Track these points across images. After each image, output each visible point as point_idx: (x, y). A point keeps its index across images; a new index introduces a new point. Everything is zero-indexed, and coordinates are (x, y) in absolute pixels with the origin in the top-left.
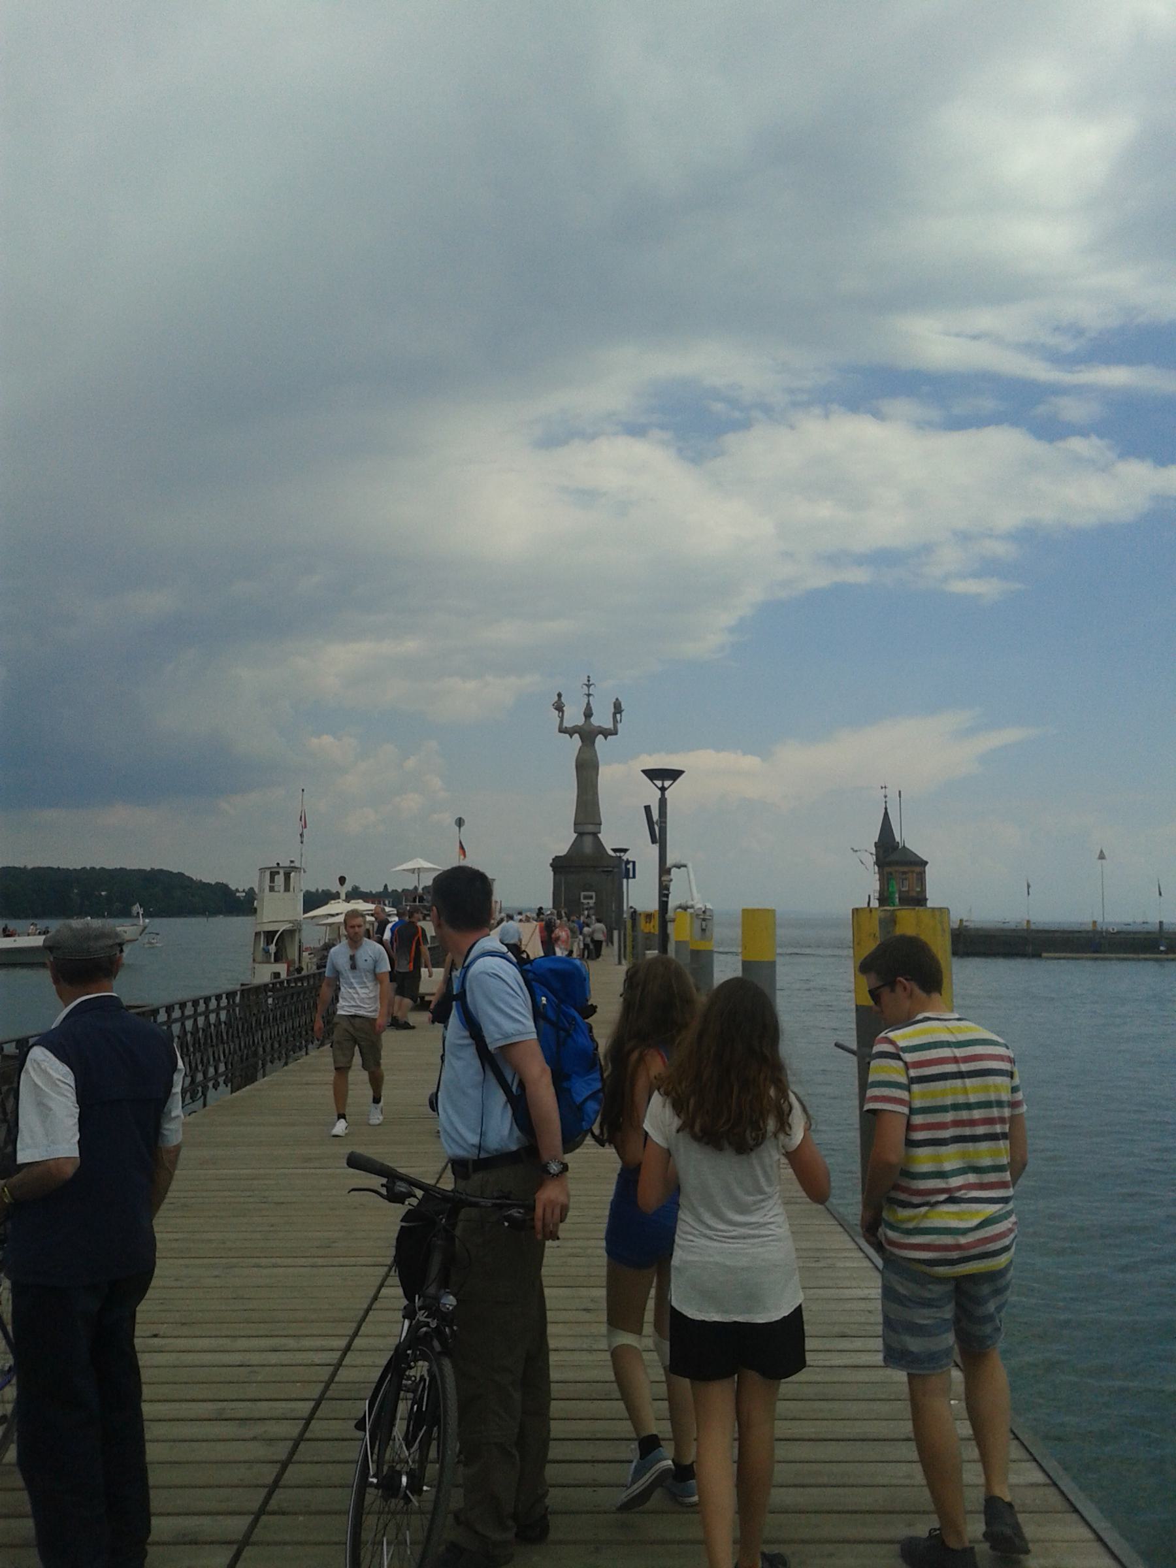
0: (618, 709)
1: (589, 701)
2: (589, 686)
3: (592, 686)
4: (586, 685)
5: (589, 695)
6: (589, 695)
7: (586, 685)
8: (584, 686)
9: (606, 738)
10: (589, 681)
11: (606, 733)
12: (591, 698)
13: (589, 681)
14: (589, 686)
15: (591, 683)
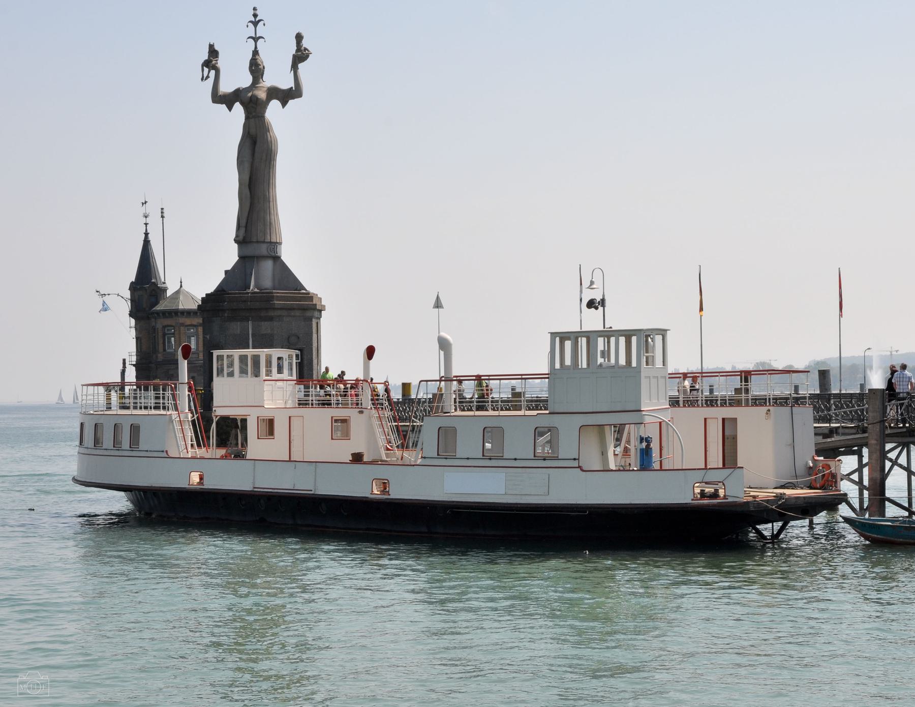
0: (300, 56)
1: (256, 47)
2: (255, 24)
3: (261, 23)
4: (250, 22)
5: (256, 39)
6: (256, 39)
7: (250, 22)
8: (251, 26)
9: (284, 104)
10: (255, 16)
11: (285, 96)
12: (260, 41)
13: (255, 16)
14: (255, 24)
15: (257, 20)
